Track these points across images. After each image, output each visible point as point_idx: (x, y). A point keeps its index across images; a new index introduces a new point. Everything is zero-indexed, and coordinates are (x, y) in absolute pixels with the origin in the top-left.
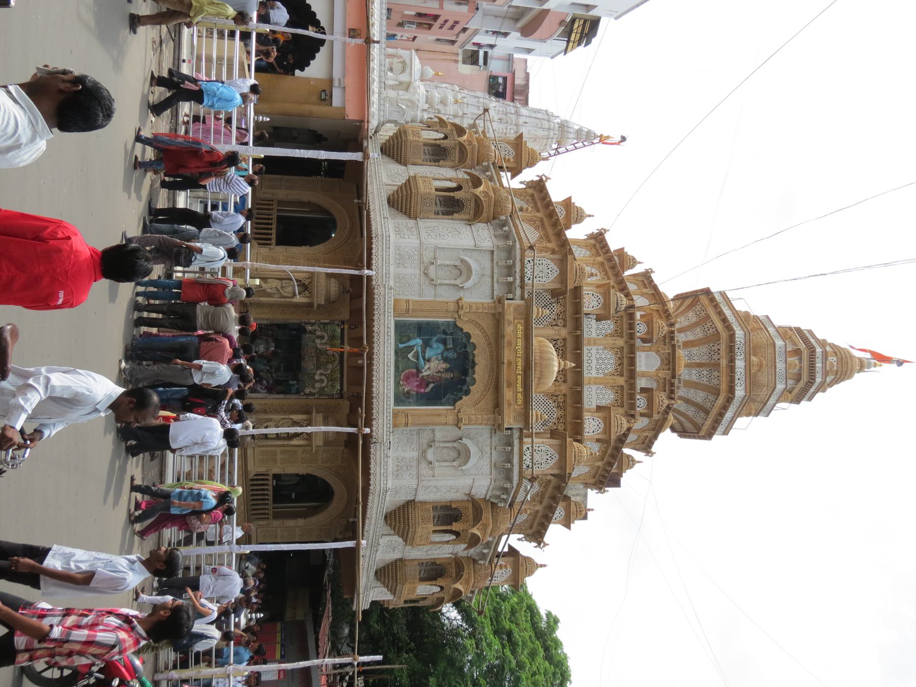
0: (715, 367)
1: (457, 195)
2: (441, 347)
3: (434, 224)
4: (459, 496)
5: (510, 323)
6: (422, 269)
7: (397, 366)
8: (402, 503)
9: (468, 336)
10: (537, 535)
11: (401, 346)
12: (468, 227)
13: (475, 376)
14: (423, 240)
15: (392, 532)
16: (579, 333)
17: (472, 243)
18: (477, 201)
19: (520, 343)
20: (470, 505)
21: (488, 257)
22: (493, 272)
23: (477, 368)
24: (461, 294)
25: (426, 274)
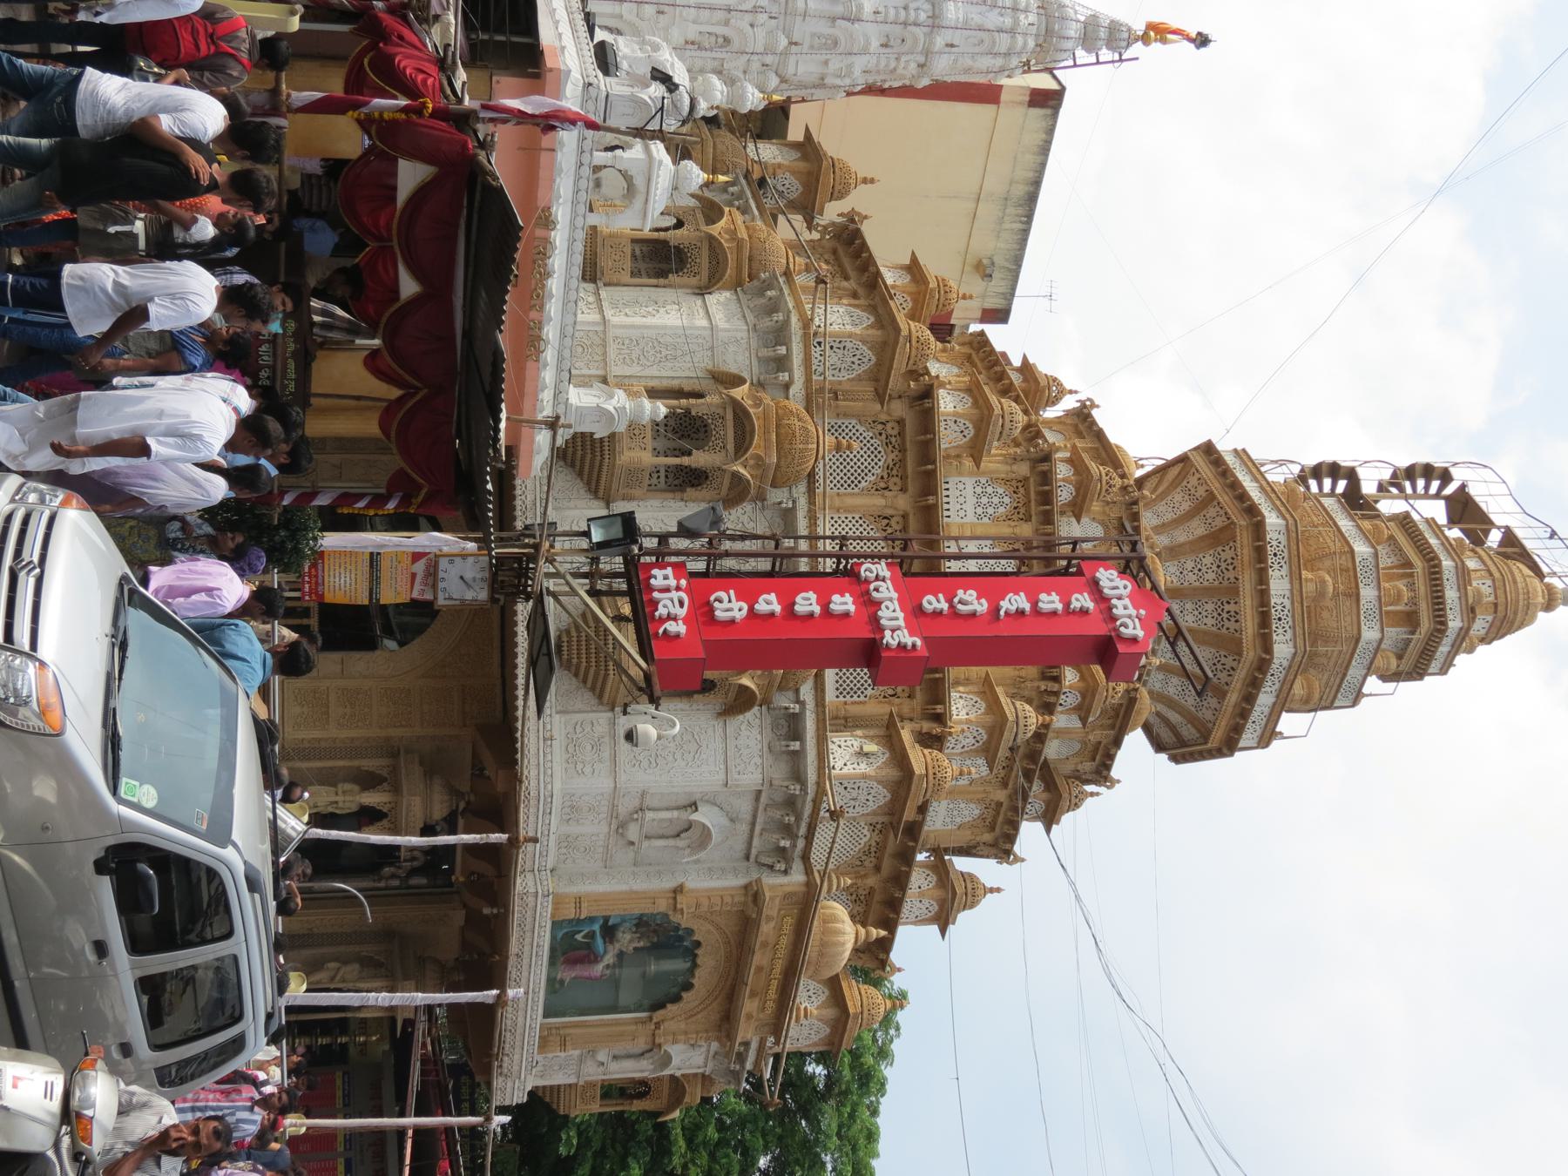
0: (1240, 608)
5: (769, 919)
9: (690, 932)
12: (718, 725)
14: (622, 778)
22: (755, 817)
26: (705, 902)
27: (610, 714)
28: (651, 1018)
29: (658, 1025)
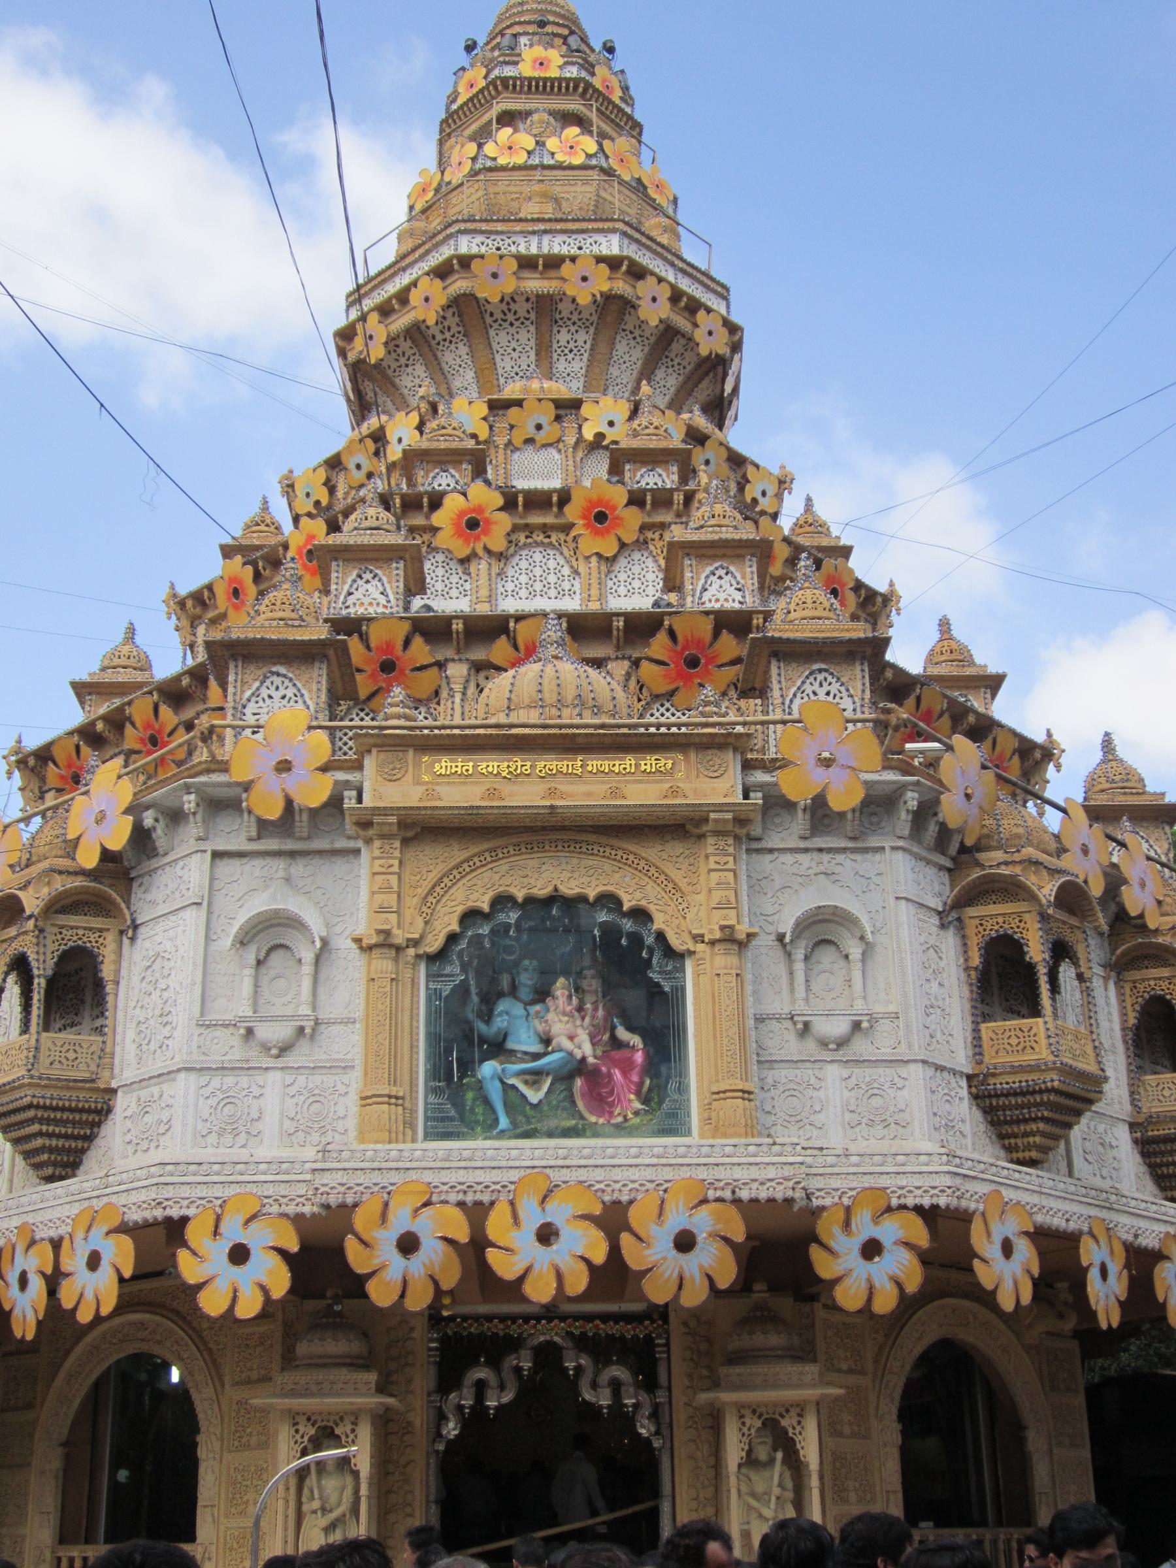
1: (42, 968)
2: (502, 1005)
3: (131, 1034)
4: (949, 941)
5: (430, 793)
6: (271, 1062)
7: (567, 1133)
8: (978, 1115)
9: (471, 916)
10: (1031, 758)
11: (504, 1122)
12: (142, 931)
13: (592, 894)
15: (1062, 1143)
16: (458, 626)
17: (190, 914)
18: (62, 905)
19: (491, 764)
20: (972, 911)
21: (228, 868)
23: (570, 888)
24: (344, 944)
25: (284, 1049)
26: (379, 898)
27: (120, 1093)
28: (691, 953)
29: (698, 938)
